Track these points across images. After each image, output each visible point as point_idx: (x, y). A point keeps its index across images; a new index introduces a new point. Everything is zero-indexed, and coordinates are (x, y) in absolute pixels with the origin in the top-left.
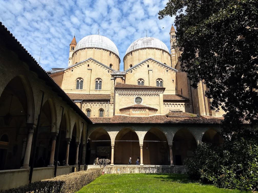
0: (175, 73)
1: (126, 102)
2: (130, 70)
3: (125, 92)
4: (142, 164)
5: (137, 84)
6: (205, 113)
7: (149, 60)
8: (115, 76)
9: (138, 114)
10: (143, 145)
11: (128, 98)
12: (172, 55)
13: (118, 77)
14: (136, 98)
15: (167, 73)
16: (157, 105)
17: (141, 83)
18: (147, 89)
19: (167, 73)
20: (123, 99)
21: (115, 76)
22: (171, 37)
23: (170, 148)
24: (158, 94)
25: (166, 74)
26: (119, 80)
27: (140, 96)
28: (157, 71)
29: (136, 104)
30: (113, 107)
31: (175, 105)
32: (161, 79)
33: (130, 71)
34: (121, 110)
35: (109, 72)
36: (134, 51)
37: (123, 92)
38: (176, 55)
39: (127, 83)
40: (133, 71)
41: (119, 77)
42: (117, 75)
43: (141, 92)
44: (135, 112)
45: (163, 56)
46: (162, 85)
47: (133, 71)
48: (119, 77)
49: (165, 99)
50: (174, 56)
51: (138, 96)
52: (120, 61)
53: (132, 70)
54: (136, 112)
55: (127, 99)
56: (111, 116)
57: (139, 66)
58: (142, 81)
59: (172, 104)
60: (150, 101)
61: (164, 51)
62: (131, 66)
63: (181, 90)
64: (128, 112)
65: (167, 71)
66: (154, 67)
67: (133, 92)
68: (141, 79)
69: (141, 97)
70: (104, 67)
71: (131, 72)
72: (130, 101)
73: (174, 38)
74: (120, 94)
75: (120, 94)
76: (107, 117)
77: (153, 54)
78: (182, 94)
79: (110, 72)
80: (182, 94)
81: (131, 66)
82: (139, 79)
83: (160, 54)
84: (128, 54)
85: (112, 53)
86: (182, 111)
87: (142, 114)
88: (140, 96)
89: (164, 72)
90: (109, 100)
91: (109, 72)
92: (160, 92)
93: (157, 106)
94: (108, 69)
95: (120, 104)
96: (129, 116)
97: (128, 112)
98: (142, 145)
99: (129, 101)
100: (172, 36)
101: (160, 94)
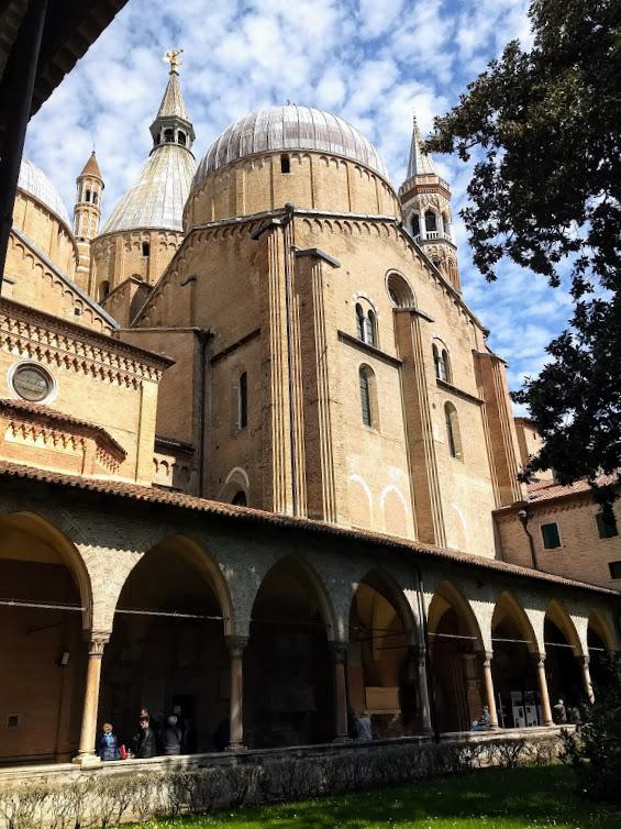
4: (89, 758)
6: (290, 506)
9: (38, 455)
10: (113, 636)
14: (24, 368)
22: (84, 195)
23: (237, 652)
24: (138, 380)
27: (45, 360)
38: (95, 270)
44: (19, 439)
50: (85, 273)
60: (92, 402)
83: (48, 231)
92: (147, 375)
98: (108, 637)
100: (88, 193)
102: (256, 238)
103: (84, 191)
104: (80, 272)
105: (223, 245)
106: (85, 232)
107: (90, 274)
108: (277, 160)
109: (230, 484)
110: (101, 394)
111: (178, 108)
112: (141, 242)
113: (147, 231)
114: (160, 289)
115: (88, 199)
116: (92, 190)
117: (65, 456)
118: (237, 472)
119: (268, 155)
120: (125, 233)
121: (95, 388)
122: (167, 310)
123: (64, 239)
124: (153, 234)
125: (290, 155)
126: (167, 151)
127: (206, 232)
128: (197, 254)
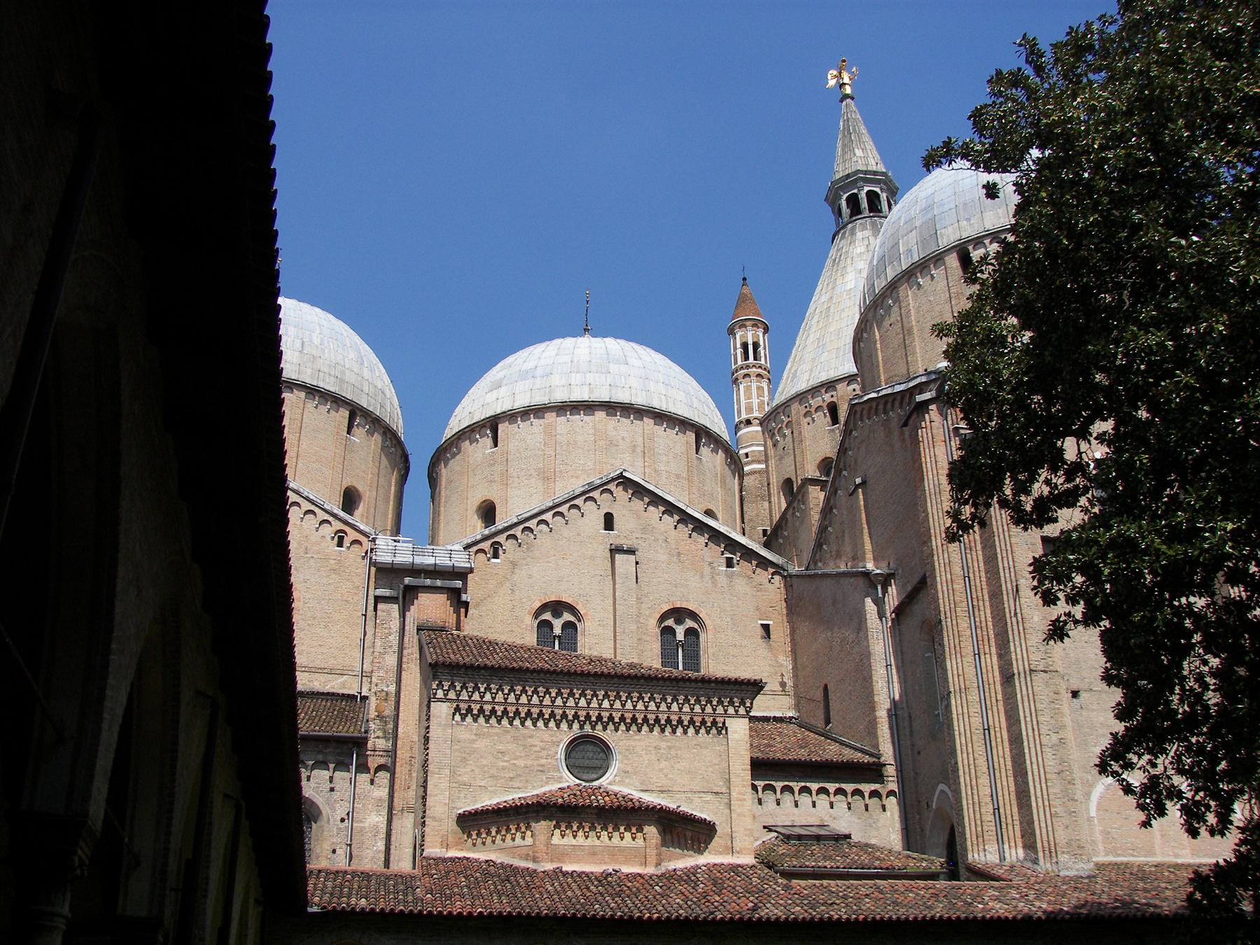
0: (777, 578)
1: (504, 768)
2: (489, 542)
3: (495, 696)
5: (530, 638)
6: (992, 848)
7: (613, 480)
8: (407, 580)
11: (515, 738)
12: (748, 464)
13: (428, 582)
14: (575, 745)
15: (730, 576)
16: (709, 797)
17: (557, 631)
18: (622, 677)
19: (730, 576)
20: (481, 744)
21: (407, 580)
24: (720, 720)
25: (723, 581)
26: (431, 607)
27: (599, 727)
28: (664, 557)
29: (570, 780)
30: (383, 793)
31: (867, 795)
32: (693, 616)
33: (486, 545)
34: (472, 822)
35: (340, 544)
36: (512, 416)
37: (488, 697)
38: (772, 462)
39: (472, 627)
40: (509, 545)
41: (439, 583)
42: (415, 571)
43: (599, 703)
45: (695, 462)
46: (693, 658)
47: (509, 545)
48: (439, 583)
49: (755, 755)
51: (588, 728)
52: (407, 469)
53: (501, 539)
54: (580, 840)
55: (512, 747)
56: (370, 859)
57: (547, 516)
58: (567, 617)
59: (832, 790)
60: (664, 764)
61: (702, 434)
62: (488, 512)
63: (819, 694)
64: (523, 838)
65: (729, 563)
66: (644, 530)
67: (551, 700)
68: (557, 607)
69: (608, 736)
70: (312, 508)
71: (496, 556)
72: (529, 763)
73: (755, 359)
74: (463, 706)
75: (463, 706)
76: (341, 862)
77: (639, 449)
78: (828, 721)
79: (347, 542)
80: (828, 721)
81: (488, 512)
82: (544, 607)
84: (470, 432)
85: (366, 414)
86: (848, 836)
87: (614, 853)
88: (599, 727)
89: (707, 570)
90: (359, 743)
91: (340, 544)
92: (731, 710)
93: (707, 802)
94: (340, 526)
95: (465, 778)
96: (531, 865)
97: (523, 838)
99: (521, 763)
100: (745, 346)
101: (729, 722)
102: (905, 424)
103: (738, 346)
104: (753, 472)
105: (886, 424)
106: (749, 409)
107: (767, 471)
108: (953, 261)
109: (938, 809)
110: (673, 752)
111: (859, 152)
112: (825, 405)
113: (830, 385)
114: (832, 502)
115: (747, 358)
116: (750, 342)
117: (621, 849)
118: (942, 791)
119: (937, 259)
120: (801, 397)
121: (663, 745)
122: (843, 532)
123: (705, 451)
124: (839, 387)
125: (970, 248)
126: (853, 233)
127: (866, 407)
128: (863, 441)
